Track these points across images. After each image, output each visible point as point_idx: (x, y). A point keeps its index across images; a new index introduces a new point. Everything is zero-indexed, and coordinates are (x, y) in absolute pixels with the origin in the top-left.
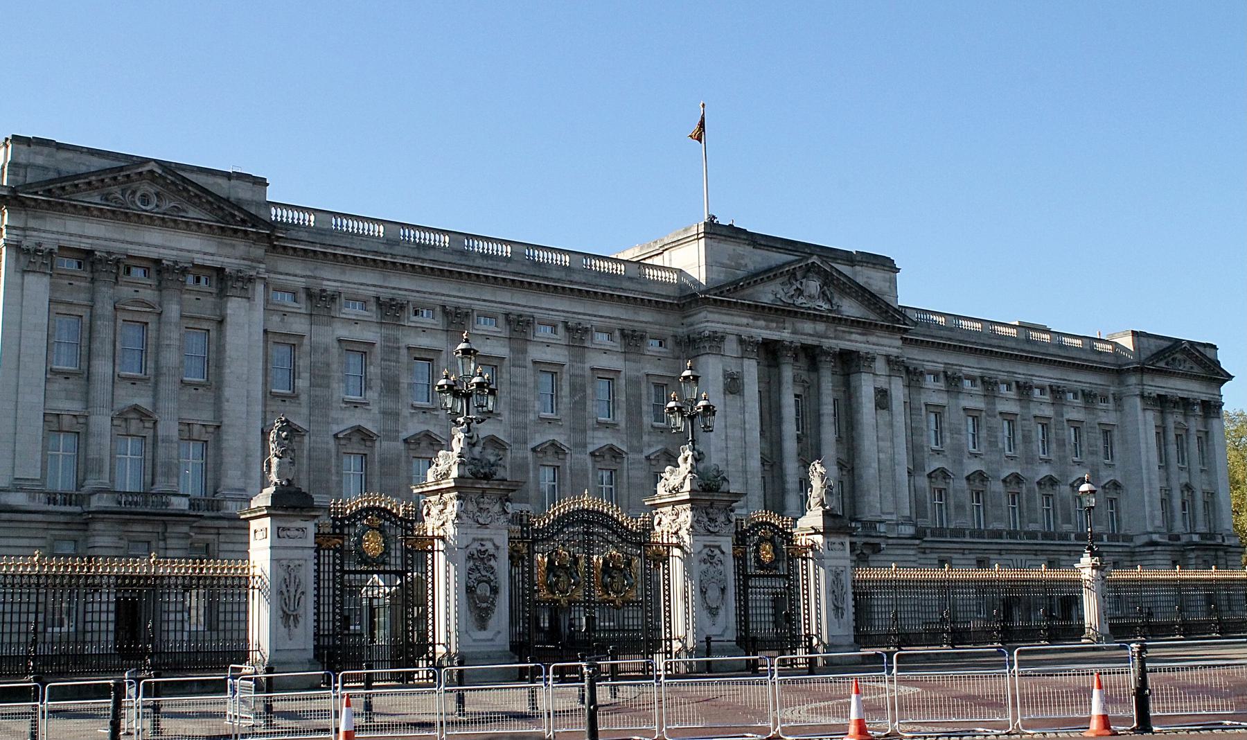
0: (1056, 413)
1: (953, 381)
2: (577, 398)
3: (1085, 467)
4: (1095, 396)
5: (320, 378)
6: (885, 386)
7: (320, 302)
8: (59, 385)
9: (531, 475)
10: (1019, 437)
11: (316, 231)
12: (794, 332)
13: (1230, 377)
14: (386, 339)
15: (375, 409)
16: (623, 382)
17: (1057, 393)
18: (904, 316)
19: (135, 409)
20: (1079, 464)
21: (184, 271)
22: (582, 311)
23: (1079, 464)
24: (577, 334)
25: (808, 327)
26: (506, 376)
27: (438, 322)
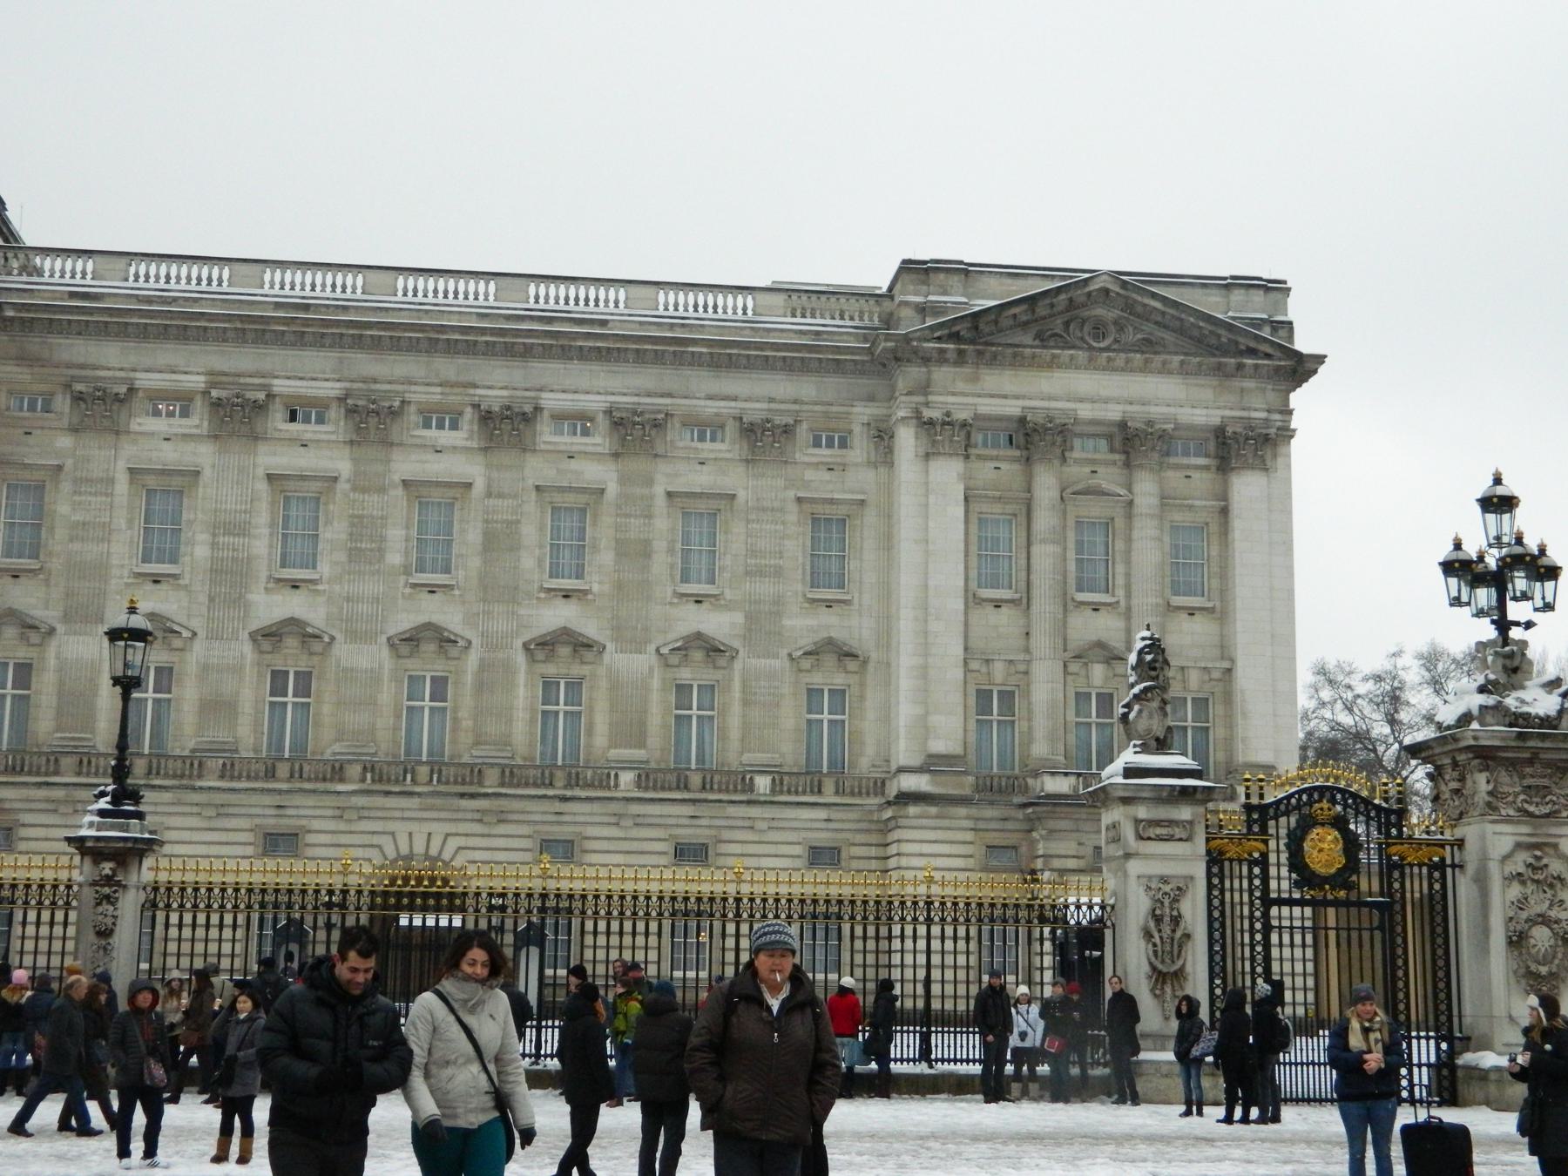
0: (623, 480)
1: (237, 414)
3: (729, 607)
4: (788, 430)
10: (468, 535)
13: (1320, 359)
17: (634, 431)
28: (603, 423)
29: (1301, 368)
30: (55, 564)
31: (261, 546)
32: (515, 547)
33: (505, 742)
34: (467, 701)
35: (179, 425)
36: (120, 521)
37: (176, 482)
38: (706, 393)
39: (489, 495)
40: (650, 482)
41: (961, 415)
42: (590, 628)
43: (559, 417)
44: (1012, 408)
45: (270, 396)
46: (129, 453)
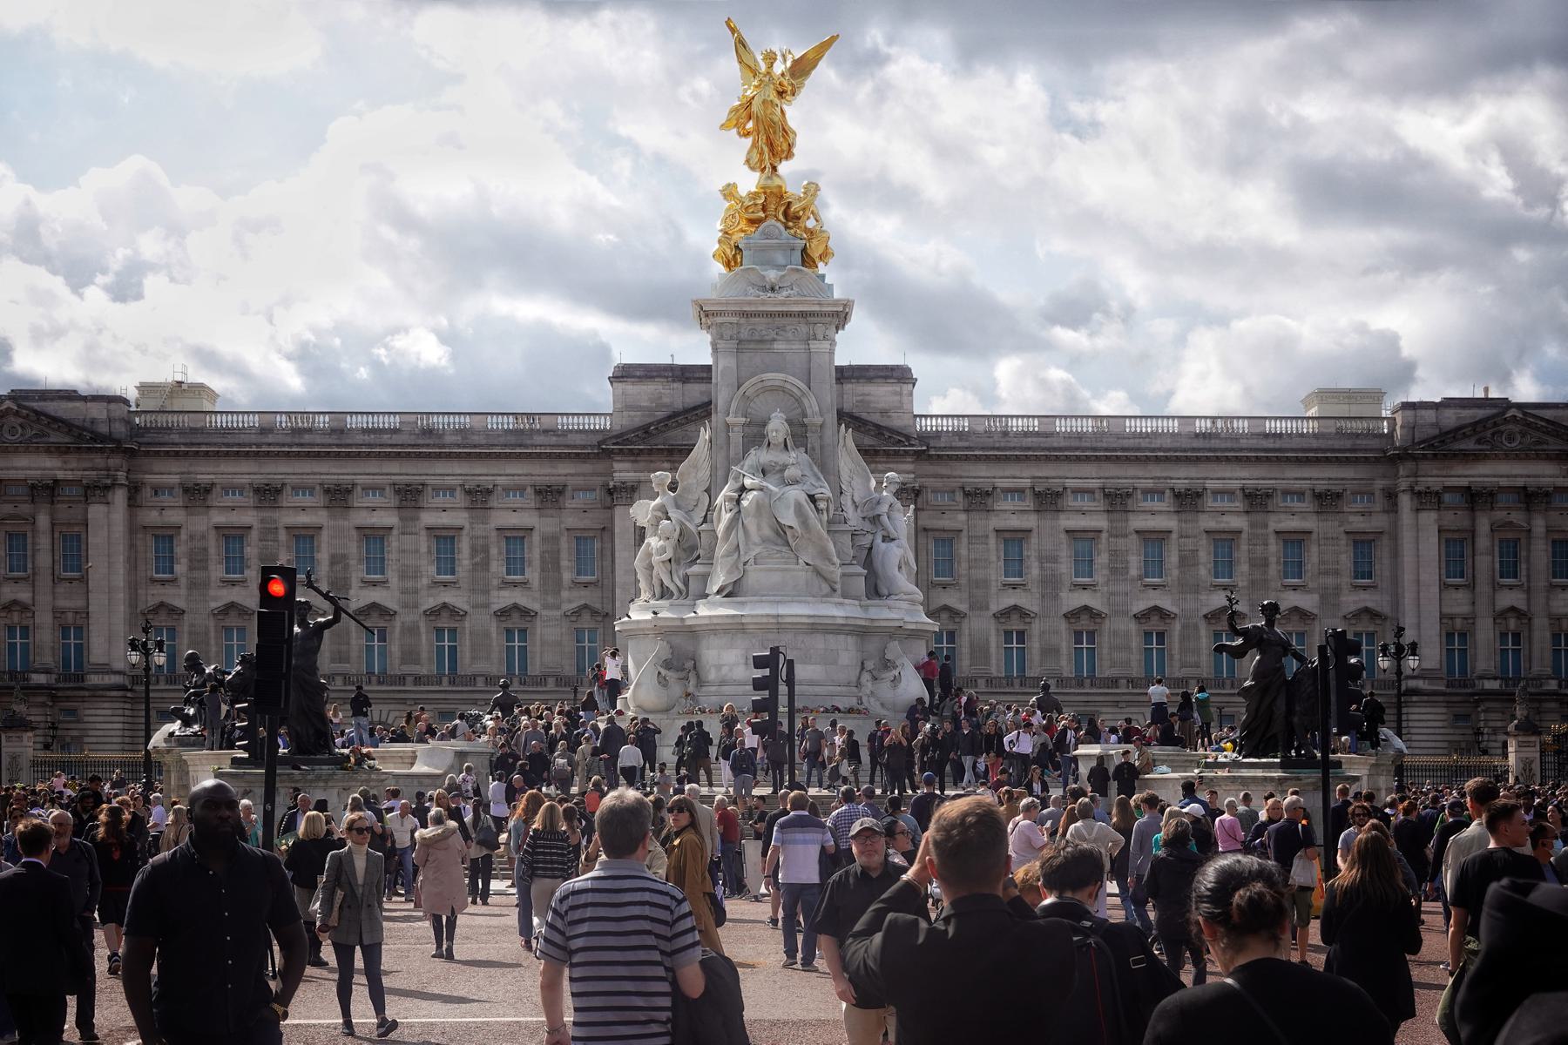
0: (1252, 525)
1: (1048, 500)
2: (478, 559)
3: (1309, 592)
4: (1339, 496)
5: (199, 560)
7: (197, 495)
9: (424, 637)
10: (1172, 558)
11: (194, 431)
14: (262, 521)
18: (908, 437)
19: (15, 602)
21: (46, 487)
22: (484, 471)
23: (1295, 588)
24: (479, 497)
26: (395, 544)
27: (319, 499)
28: (1239, 494)
30: (963, 581)
31: (1065, 568)
32: (1196, 564)
33: (1197, 666)
34: (1176, 645)
36: (993, 558)
37: (1020, 535)
40: (1266, 526)
43: (1216, 492)
44: (1464, 482)
46: (996, 522)
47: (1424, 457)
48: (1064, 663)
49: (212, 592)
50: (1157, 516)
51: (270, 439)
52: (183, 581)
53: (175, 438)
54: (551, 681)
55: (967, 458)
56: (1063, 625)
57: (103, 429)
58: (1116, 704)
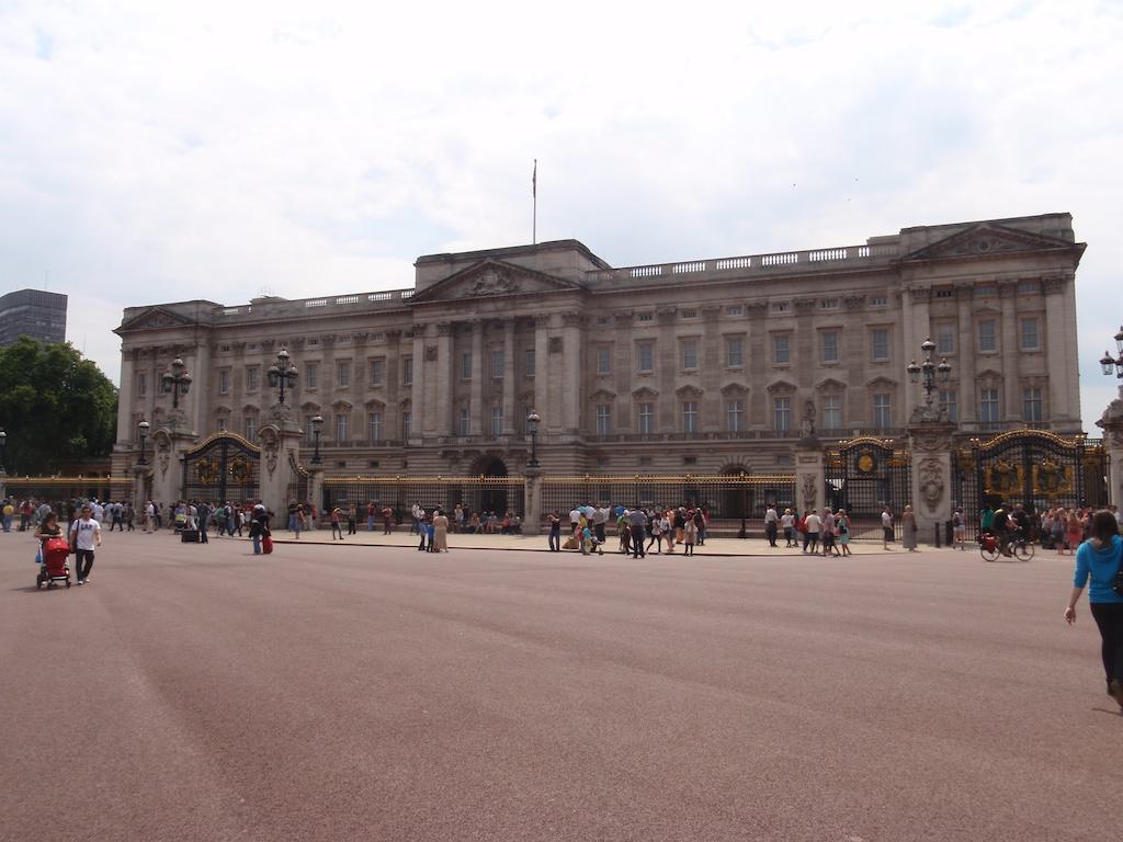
0: (800, 325)
1: (667, 318)
4: (862, 300)
5: (238, 385)
6: (559, 335)
8: (140, 403)
10: (747, 350)
12: (478, 312)
13: (1085, 245)
14: (265, 361)
15: (260, 395)
16: (387, 362)
17: (804, 308)
20: (830, 366)
23: (830, 366)
24: (361, 340)
25: (490, 306)
29: (1076, 251)
31: (677, 361)
35: (649, 323)
38: (829, 290)
39: (752, 335)
41: (926, 287)
42: (790, 381)
43: (775, 305)
44: (948, 281)
45: (676, 310)
47: (916, 266)
48: (677, 425)
49: (243, 400)
50: (737, 324)
51: (269, 316)
52: (231, 395)
53: (231, 321)
54: (388, 443)
55: (616, 295)
56: (676, 397)
57: (194, 317)
58: (707, 450)
